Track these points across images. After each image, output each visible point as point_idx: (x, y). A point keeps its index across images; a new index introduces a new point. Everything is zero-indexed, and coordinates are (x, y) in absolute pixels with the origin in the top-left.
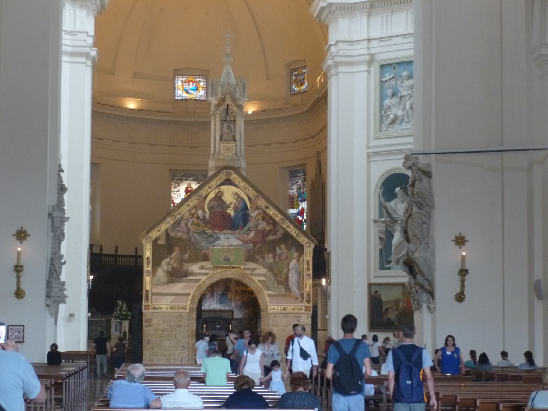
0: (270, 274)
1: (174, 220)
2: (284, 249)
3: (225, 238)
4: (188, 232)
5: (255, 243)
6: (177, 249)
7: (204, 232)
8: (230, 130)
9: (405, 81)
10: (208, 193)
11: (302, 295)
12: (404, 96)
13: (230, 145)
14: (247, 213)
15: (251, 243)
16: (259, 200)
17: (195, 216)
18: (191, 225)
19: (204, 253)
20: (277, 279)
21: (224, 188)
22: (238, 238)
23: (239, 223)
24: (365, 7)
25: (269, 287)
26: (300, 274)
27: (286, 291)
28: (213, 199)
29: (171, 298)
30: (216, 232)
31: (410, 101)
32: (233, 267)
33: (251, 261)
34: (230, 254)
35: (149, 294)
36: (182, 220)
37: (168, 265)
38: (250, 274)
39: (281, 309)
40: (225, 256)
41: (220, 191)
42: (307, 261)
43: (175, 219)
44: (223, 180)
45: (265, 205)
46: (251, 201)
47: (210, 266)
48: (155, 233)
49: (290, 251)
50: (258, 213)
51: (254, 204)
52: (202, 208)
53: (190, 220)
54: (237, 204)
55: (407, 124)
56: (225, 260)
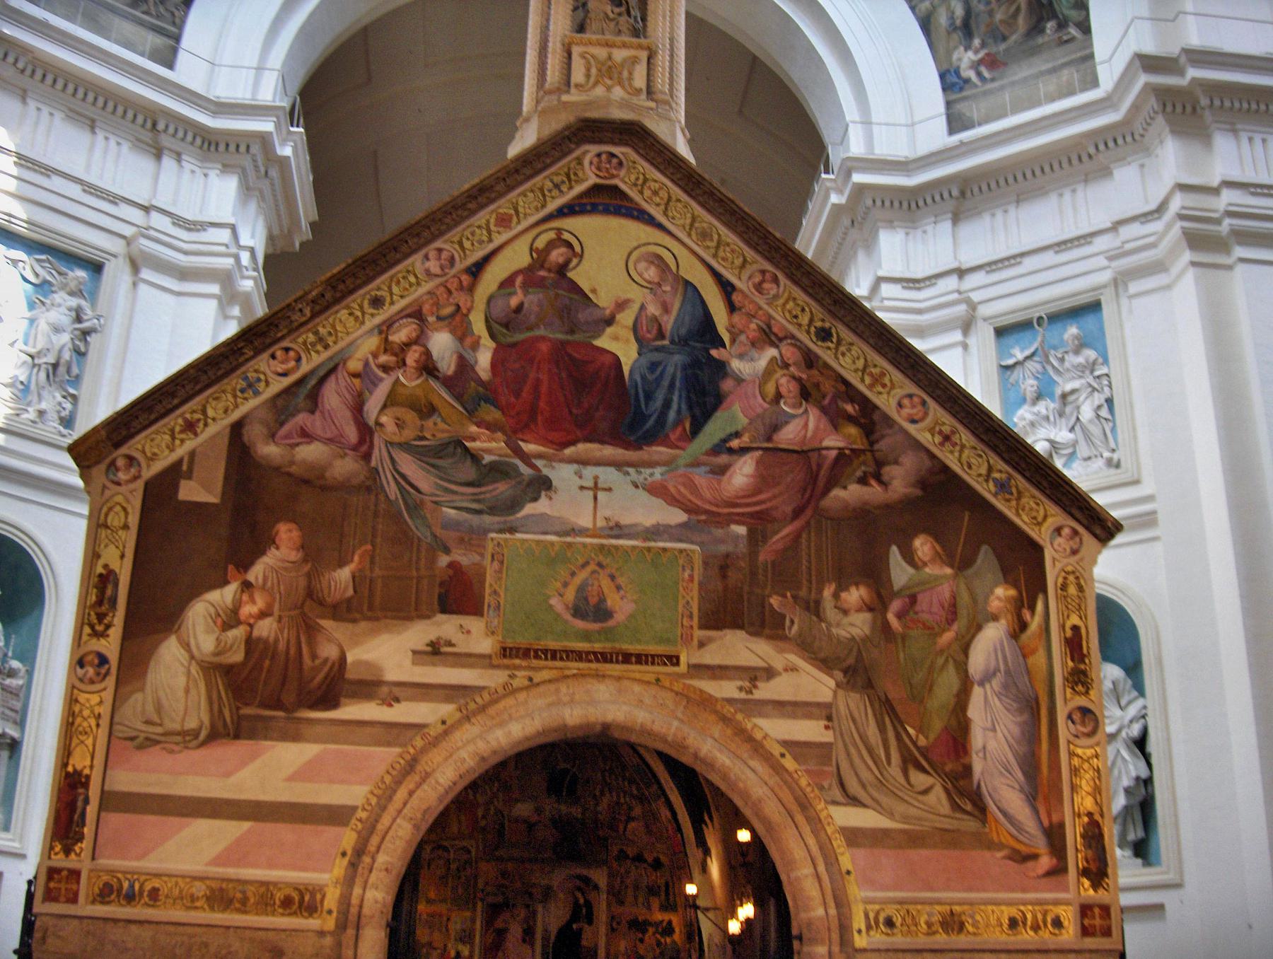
0: (853, 704)
1: (284, 375)
2: (933, 560)
3: (582, 488)
4: (361, 441)
5: (760, 523)
6: (287, 533)
7: (457, 445)
8: (623, 9)
9: (1071, 354)
10: (491, 247)
11: (1055, 836)
12: (1073, 391)
13: (619, 55)
14: (710, 357)
16: (776, 297)
17: (412, 357)
18: (385, 407)
19: (452, 565)
20: (898, 738)
21: (582, 226)
22: (657, 490)
23: (667, 404)
24: (946, 195)
25: (854, 787)
27: (955, 807)
28: (519, 280)
29: (232, 830)
30: (529, 447)
31: (1093, 402)
32: (627, 658)
33: (736, 625)
34: (612, 577)
35: (87, 801)
36: (332, 378)
37: (226, 626)
38: (730, 701)
39: (929, 925)
40: (581, 589)
41: (559, 241)
42: (1069, 633)
43: (297, 367)
44: (579, 189)
45: (809, 325)
46: (736, 298)
47: (485, 645)
48: (167, 437)
49: (970, 571)
50: (773, 359)
51: (752, 316)
52: (458, 323)
53: (381, 380)
54: (653, 309)
55: (1089, 463)
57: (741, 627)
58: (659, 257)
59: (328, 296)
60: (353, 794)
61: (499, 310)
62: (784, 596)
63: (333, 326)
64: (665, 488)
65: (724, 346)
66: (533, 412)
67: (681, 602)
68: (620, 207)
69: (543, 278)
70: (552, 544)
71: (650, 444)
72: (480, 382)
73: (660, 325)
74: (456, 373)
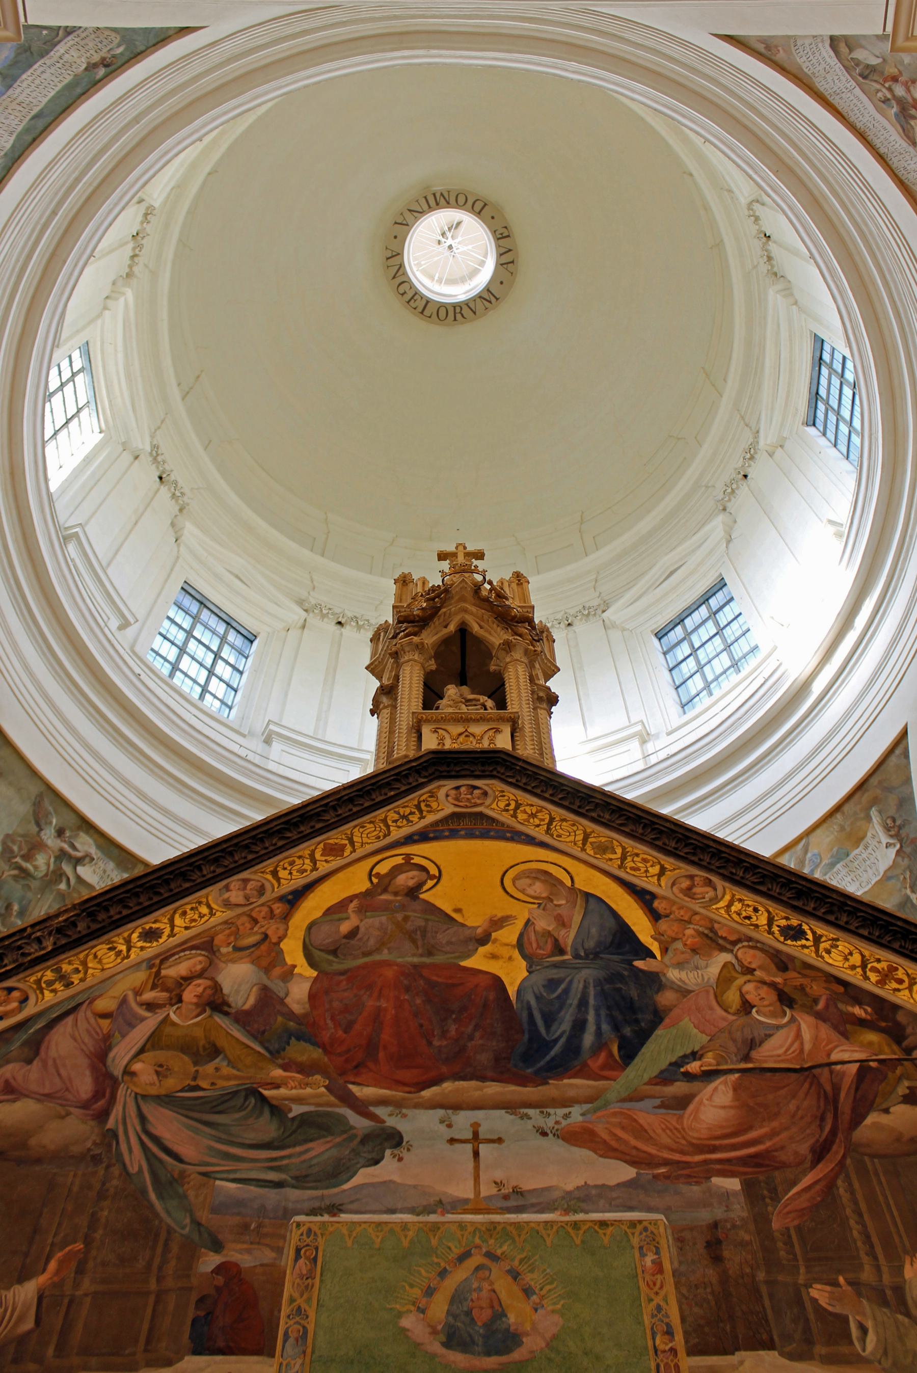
3: (452, 1141)
4: (97, 1095)
10: (315, 875)
15: (732, 1174)
18: (142, 1051)
23: (579, 1026)
34: (515, 1275)
36: (70, 1020)
40: (457, 1298)
43: (20, 1010)
53: (143, 1019)
54: (543, 924)
57: (769, 1345)
58: (546, 873)
59: (81, 926)
61: (324, 936)
62: (835, 1284)
63: (84, 963)
64: (592, 1133)
65: (654, 957)
66: (371, 1047)
67: (648, 1309)
68: (489, 831)
69: (390, 902)
70: (405, 1226)
71: (560, 1077)
72: (291, 1015)
73: (556, 940)
74: (255, 1006)
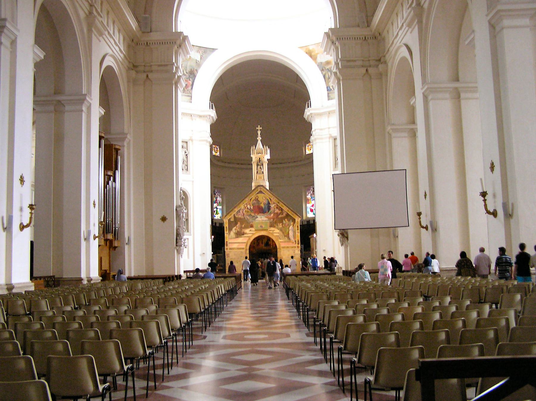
11: (295, 241)
17: (246, 208)
21: (258, 195)
22: (266, 217)
26: (294, 232)
29: (237, 244)
30: (256, 214)
56: (260, 227)
60: (246, 241)
